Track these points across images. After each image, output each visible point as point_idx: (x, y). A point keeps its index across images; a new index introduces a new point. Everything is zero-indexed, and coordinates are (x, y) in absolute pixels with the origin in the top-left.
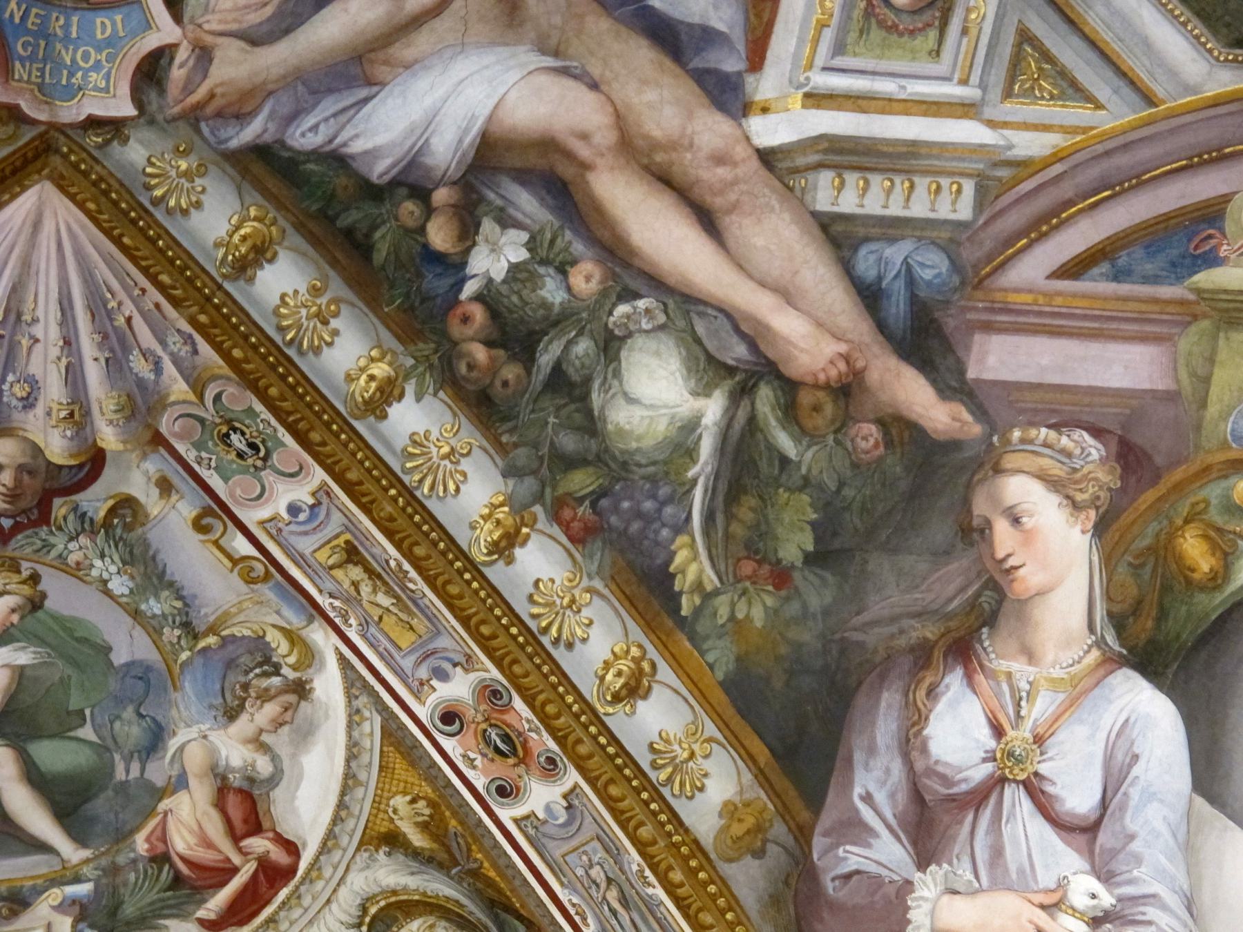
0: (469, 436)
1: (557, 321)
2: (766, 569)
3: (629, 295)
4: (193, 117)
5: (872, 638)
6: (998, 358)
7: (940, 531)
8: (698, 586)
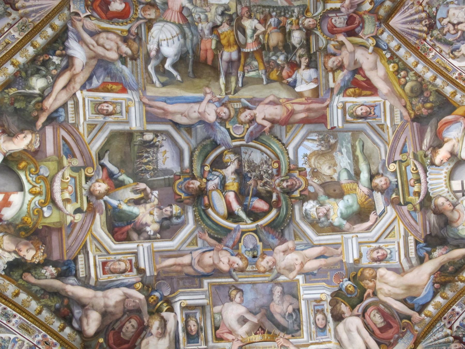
0: (29, 58)
1: (47, 69)
2: (13, 101)
3: (52, 78)
4: (71, 19)
5: (4, 118)
6: (49, 131)
7: (22, 126)
8: (10, 92)
